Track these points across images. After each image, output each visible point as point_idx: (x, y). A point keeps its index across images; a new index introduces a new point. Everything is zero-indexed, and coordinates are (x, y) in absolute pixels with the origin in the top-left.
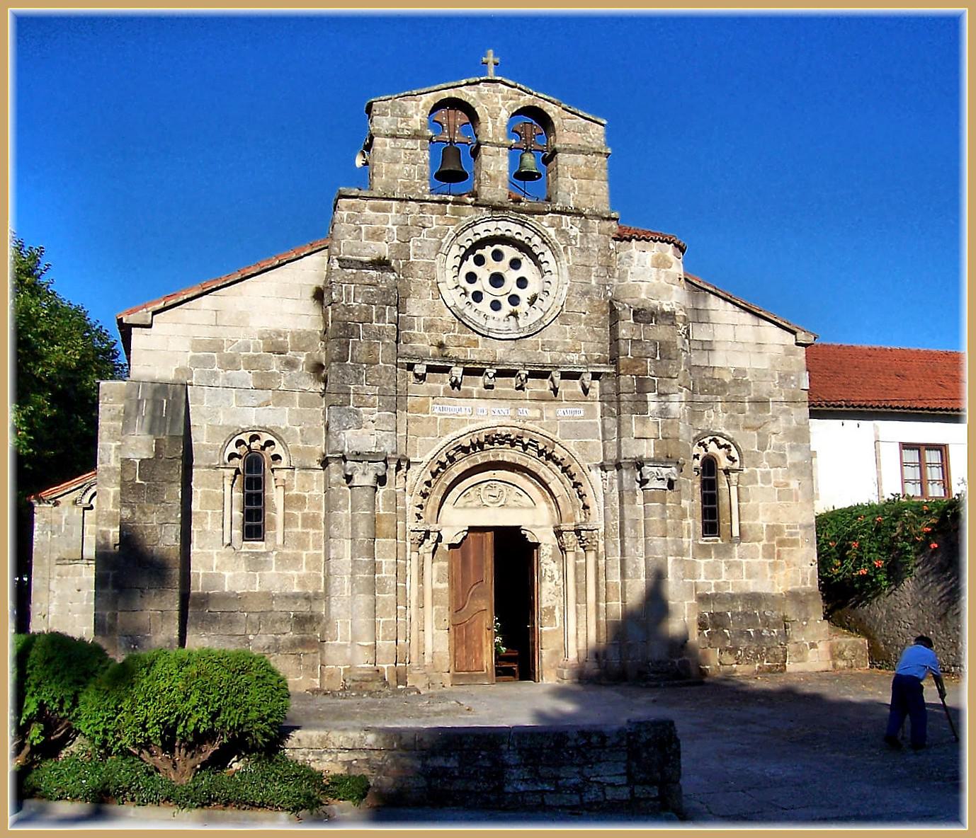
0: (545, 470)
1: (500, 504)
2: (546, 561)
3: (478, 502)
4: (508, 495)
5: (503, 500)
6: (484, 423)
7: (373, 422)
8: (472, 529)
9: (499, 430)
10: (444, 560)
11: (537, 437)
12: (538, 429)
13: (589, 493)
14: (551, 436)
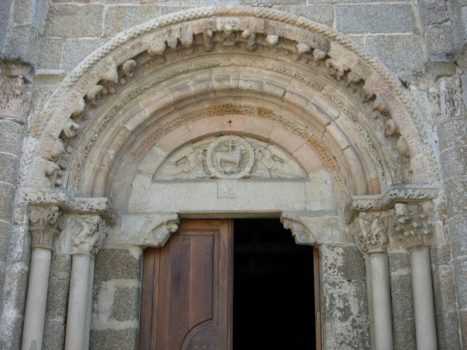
2: (331, 280)
3: (200, 173)
5: (248, 169)
6: (189, 11)
9: (221, 24)
10: (128, 276)
11: (293, 33)
12: (293, 16)
13: (408, 130)
14: (321, 27)
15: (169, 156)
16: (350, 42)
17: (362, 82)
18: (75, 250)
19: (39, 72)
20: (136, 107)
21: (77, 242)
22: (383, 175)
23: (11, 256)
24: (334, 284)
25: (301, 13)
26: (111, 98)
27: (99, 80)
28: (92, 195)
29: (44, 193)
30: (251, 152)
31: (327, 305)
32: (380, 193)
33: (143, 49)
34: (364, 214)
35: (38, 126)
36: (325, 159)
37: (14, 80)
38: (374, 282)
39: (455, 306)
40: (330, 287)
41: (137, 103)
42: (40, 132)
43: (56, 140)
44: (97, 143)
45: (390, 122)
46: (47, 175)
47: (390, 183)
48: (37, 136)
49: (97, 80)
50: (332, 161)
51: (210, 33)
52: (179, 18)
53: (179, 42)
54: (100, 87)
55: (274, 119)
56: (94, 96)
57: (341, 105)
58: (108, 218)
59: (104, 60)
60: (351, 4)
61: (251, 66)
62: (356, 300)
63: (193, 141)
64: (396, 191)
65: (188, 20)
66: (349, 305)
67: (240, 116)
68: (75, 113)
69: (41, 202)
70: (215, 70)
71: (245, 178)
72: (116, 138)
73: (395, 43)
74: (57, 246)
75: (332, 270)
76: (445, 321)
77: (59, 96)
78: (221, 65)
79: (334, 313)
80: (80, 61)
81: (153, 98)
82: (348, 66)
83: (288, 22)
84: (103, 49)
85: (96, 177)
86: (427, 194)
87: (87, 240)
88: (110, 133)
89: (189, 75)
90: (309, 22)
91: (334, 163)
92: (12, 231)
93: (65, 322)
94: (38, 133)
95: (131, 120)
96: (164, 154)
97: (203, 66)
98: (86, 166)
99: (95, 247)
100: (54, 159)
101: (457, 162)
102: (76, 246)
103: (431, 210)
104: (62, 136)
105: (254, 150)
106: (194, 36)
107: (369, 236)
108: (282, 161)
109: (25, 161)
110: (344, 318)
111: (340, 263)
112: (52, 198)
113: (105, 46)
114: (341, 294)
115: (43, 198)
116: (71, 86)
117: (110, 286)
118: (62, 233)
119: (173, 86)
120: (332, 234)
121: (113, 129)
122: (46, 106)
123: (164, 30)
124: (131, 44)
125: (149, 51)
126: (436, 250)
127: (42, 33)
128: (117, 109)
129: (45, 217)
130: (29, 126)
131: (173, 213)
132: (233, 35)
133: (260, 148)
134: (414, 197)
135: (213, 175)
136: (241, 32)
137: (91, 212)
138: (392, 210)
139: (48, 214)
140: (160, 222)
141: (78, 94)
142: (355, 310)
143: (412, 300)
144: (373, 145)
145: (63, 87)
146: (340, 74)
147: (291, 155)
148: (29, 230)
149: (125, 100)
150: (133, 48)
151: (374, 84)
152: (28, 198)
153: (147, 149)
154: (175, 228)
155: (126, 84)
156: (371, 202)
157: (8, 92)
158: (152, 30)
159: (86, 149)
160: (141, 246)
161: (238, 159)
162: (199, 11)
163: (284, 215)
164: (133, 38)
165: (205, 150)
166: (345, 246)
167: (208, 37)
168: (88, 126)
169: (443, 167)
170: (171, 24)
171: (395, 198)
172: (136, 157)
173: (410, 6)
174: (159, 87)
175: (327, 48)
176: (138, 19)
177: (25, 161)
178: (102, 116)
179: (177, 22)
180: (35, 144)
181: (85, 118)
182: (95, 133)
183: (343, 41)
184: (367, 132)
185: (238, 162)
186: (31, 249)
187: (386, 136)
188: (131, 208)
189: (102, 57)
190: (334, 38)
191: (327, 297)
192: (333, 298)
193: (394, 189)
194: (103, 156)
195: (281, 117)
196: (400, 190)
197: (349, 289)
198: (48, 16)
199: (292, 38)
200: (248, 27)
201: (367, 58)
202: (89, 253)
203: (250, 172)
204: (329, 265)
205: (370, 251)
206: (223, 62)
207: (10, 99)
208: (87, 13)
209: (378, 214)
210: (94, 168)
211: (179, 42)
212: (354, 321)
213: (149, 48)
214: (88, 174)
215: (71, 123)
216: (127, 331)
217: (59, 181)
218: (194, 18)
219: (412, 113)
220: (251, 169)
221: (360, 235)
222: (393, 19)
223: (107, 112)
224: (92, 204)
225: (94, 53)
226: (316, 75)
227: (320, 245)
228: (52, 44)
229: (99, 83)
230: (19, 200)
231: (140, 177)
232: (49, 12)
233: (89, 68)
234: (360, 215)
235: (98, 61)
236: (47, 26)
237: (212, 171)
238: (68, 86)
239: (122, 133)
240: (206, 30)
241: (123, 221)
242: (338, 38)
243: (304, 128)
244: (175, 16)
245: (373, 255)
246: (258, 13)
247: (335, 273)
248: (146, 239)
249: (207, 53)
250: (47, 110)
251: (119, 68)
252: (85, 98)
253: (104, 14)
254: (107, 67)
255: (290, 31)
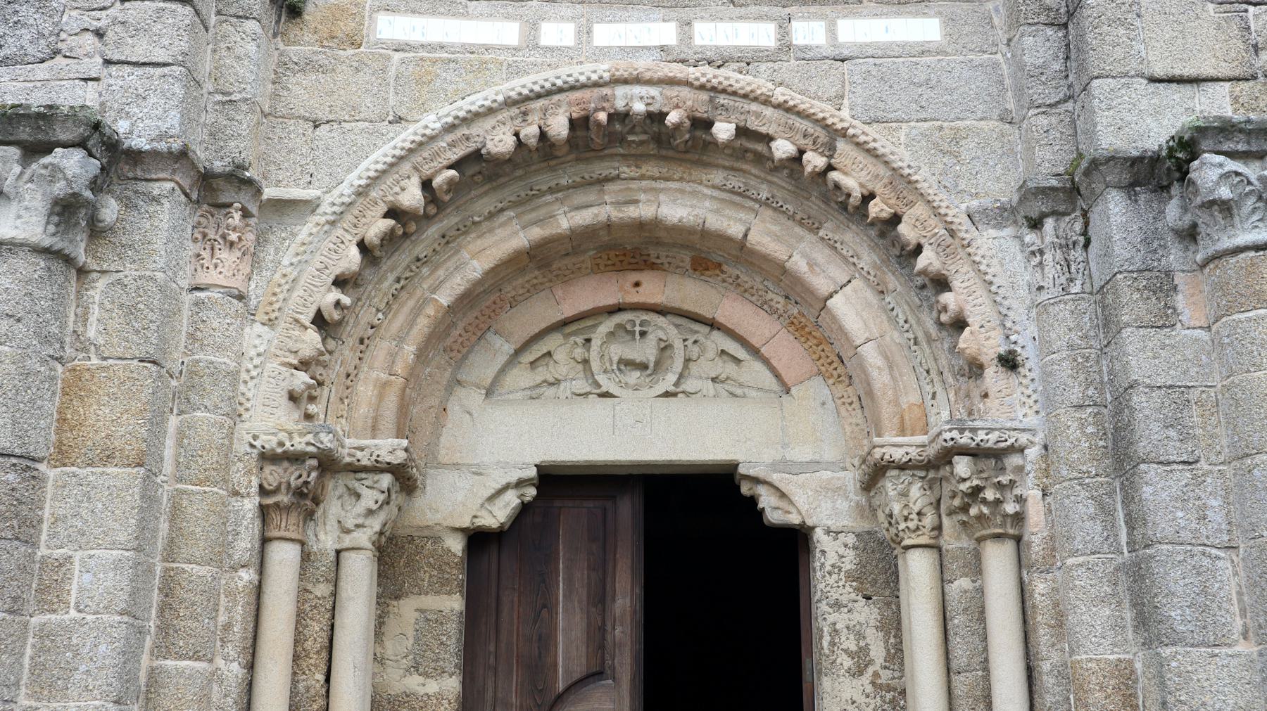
0: (811, 258)
1: (660, 389)
2: (834, 595)
4: (688, 361)
5: (671, 378)
7: (99, 34)
8: (557, 484)
10: (441, 586)
11: (765, 120)
14: (822, 109)
15: (518, 352)
16: (874, 140)
17: (896, 219)
18: (347, 541)
19: (269, 192)
20: (456, 258)
21: (350, 523)
22: (934, 397)
23: (230, 556)
24: (837, 605)
25: (779, 80)
26: (408, 242)
27: (386, 209)
28: (374, 431)
29: (290, 434)
30: (678, 344)
31: (825, 644)
32: (926, 434)
33: (471, 147)
34: (895, 473)
35: (271, 304)
36: (822, 361)
37: (224, 211)
38: (913, 600)
39: (1063, 650)
40: (831, 610)
41: (457, 252)
42: (276, 314)
43: (306, 328)
44: (382, 331)
45: (947, 298)
46: (293, 397)
47: (945, 415)
48: (271, 323)
49: (383, 208)
50: (835, 365)
51: (602, 116)
52: (543, 87)
53: (543, 135)
54: (390, 222)
55: (724, 281)
56: (377, 241)
57: (855, 260)
58: (404, 479)
59: (395, 169)
60: (878, 61)
61: (681, 179)
62: (881, 635)
63: (565, 323)
64: (955, 434)
65: (561, 90)
66: (867, 645)
67: (656, 273)
68: (343, 274)
69: (285, 452)
70: (610, 187)
71: (667, 394)
72: (419, 320)
73: (963, 143)
74: (312, 537)
75: (835, 576)
76: (1045, 678)
77: (311, 243)
78: (623, 176)
79: (839, 661)
80: (349, 171)
81: (488, 240)
82: (870, 187)
83: (755, 99)
84: (395, 148)
85: (381, 397)
86: (1013, 440)
87: (367, 522)
88: (406, 309)
89: (560, 195)
90: (795, 99)
91: (840, 370)
92: (230, 508)
93: (328, 680)
94: (273, 316)
95: (448, 285)
96: (508, 348)
97: (587, 176)
98: (362, 376)
99: (381, 533)
100: (304, 365)
101: (1069, 382)
102: (348, 532)
103: (1020, 469)
104: (320, 320)
105: (685, 340)
106: (571, 121)
107: (906, 513)
108: (737, 361)
109: (248, 371)
110: (858, 672)
111: (848, 566)
112: (308, 444)
113: (398, 141)
114: (852, 623)
115: (288, 444)
116: (333, 223)
117: (408, 609)
118: (320, 512)
119: (527, 217)
120: (834, 508)
121: (411, 303)
122: (285, 262)
123: (514, 111)
124: (449, 138)
125: (484, 151)
126: (1029, 545)
127: (267, 110)
128: (419, 264)
129: (293, 478)
130: (253, 302)
131: (525, 466)
132: (648, 122)
133: (695, 337)
134: (988, 445)
135: (604, 389)
136: (662, 116)
137: (378, 468)
138: (948, 468)
139: (297, 473)
140: (504, 482)
141: (349, 237)
142: (878, 653)
143: (985, 639)
144: (915, 339)
145: (318, 224)
146: (855, 199)
147: (755, 352)
148: (261, 506)
149: (436, 246)
150: (452, 145)
151: (918, 224)
152: (258, 443)
153: (474, 338)
154: (531, 492)
155: (436, 214)
156: (910, 450)
157: (212, 237)
158: (490, 111)
159: (362, 341)
160: (463, 530)
161: (652, 359)
162: (582, 74)
163: (742, 470)
164: (451, 128)
165: (588, 340)
166: (859, 530)
167: (598, 124)
168: (364, 297)
169: (1045, 389)
170: (527, 99)
171: (953, 447)
172: (452, 355)
173: (996, 65)
174: (503, 218)
175: (830, 149)
176: (461, 86)
177: (248, 371)
178: (391, 278)
179: (539, 96)
180: (266, 337)
181: (359, 281)
182: (378, 310)
183: (862, 138)
184: (904, 312)
185: (651, 365)
186: (265, 541)
187: (941, 325)
188: (444, 456)
189: (392, 165)
190: (843, 133)
191: (825, 629)
192: (836, 631)
193: (950, 430)
194: (393, 356)
195: (738, 277)
196: (962, 431)
197: (866, 614)
198: (276, 72)
199: (763, 130)
200: (677, 107)
201: (907, 171)
202: (369, 545)
203: (677, 384)
204: (828, 568)
205: (907, 542)
206: (625, 169)
207: (217, 251)
208: (357, 70)
209: (922, 474)
210: (378, 379)
211: (543, 135)
212: (876, 674)
213: (484, 146)
214: (365, 391)
215: (335, 295)
216: (439, 697)
217: (312, 408)
218: (572, 88)
219: (991, 283)
220: (679, 379)
221: (887, 511)
222: (962, 90)
223: (400, 269)
224: (377, 453)
225: (377, 155)
226: (808, 199)
227: (813, 528)
228: (289, 133)
229: (386, 216)
230: (241, 448)
231: (460, 392)
232: (278, 65)
233: (368, 185)
234: (888, 474)
235: (384, 172)
236: (276, 96)
237: (601, 382)
238: (328, 222)
239: (430, 311)
240: (596, 110)
241: (428, 482)
242: (851, 132)
243: (782, 300)
244: (535, 83)
245: (912, 551)
246: (697, 79)
247: (841, 584)
248: (475, 517)
249: (592, 154)
250: (289, 269)
251: (426, 185)
252: (362, 246)
253: (392, 72)
254: (402, 183)
255: (758, 115)
